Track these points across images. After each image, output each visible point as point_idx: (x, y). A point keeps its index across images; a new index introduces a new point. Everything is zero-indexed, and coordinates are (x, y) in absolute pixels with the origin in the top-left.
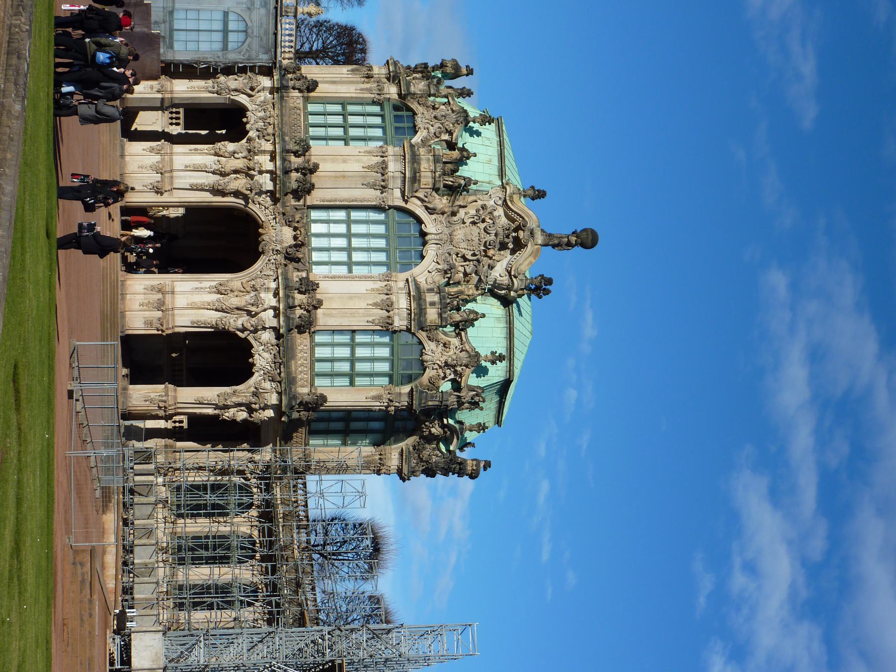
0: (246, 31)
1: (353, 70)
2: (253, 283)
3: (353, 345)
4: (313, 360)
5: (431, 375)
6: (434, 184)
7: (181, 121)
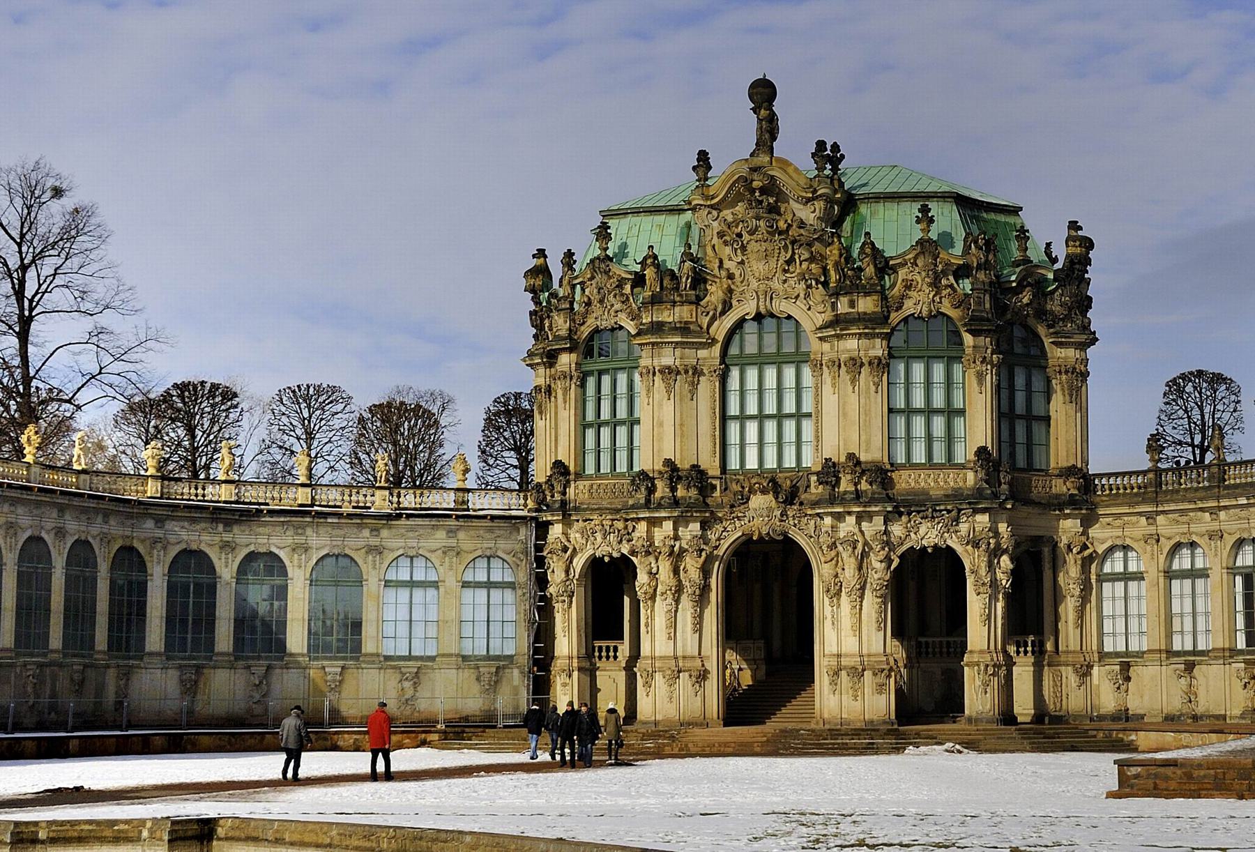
0: (489, 558)
1: (541, 413)
2: (824, 547)
3: (909, 412)
4: (930, 464)
5: (949, 306)
6: (691, 303)
7: (612, 644)
